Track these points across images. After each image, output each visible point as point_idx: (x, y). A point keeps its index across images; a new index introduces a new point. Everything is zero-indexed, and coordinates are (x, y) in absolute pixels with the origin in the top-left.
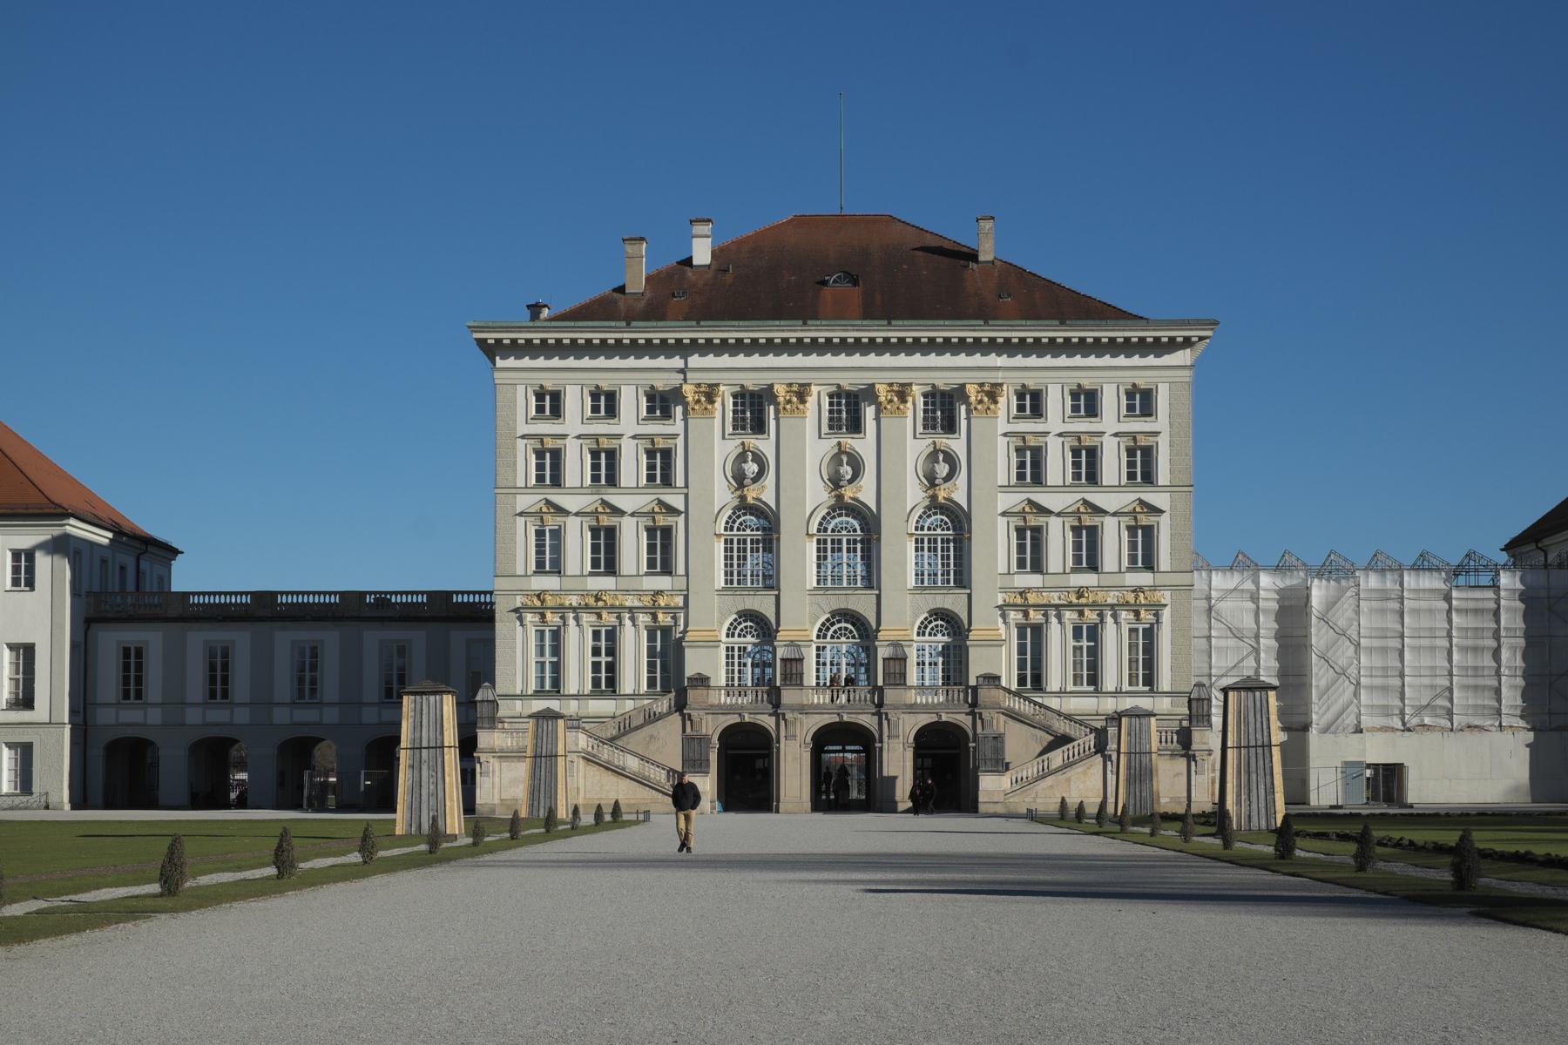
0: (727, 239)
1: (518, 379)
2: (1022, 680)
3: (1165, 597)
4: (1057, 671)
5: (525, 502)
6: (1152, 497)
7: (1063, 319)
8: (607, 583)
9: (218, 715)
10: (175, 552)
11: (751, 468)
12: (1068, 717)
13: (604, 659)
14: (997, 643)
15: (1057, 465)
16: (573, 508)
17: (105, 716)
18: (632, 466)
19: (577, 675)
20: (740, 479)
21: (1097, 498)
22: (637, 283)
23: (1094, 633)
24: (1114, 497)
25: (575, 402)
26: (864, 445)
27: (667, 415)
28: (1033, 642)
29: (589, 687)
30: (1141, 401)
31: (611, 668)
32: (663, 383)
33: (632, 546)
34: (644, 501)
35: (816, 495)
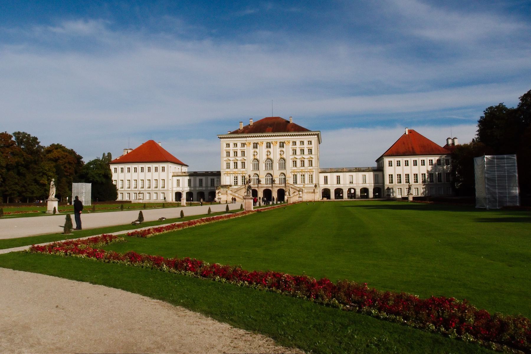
1: (224, 142)
3: (314, 170)
6: (312, 156)
7: (298, 131)
8: (236, 170)
9: (201, 189)
11: (256, 153)
14: (290, 177)
15: (298, 152)
18: (239, 154)
20: (254, 155)
22: (242, 128)
23: (304, 176)
24: (306, 156)
25: (232, 145)
26: (271, 150)
28: (295, 176)
30: (310, 142)
32: (243, 142)
33: (239, 165)
34: (241, 158)
35: (265, 157)
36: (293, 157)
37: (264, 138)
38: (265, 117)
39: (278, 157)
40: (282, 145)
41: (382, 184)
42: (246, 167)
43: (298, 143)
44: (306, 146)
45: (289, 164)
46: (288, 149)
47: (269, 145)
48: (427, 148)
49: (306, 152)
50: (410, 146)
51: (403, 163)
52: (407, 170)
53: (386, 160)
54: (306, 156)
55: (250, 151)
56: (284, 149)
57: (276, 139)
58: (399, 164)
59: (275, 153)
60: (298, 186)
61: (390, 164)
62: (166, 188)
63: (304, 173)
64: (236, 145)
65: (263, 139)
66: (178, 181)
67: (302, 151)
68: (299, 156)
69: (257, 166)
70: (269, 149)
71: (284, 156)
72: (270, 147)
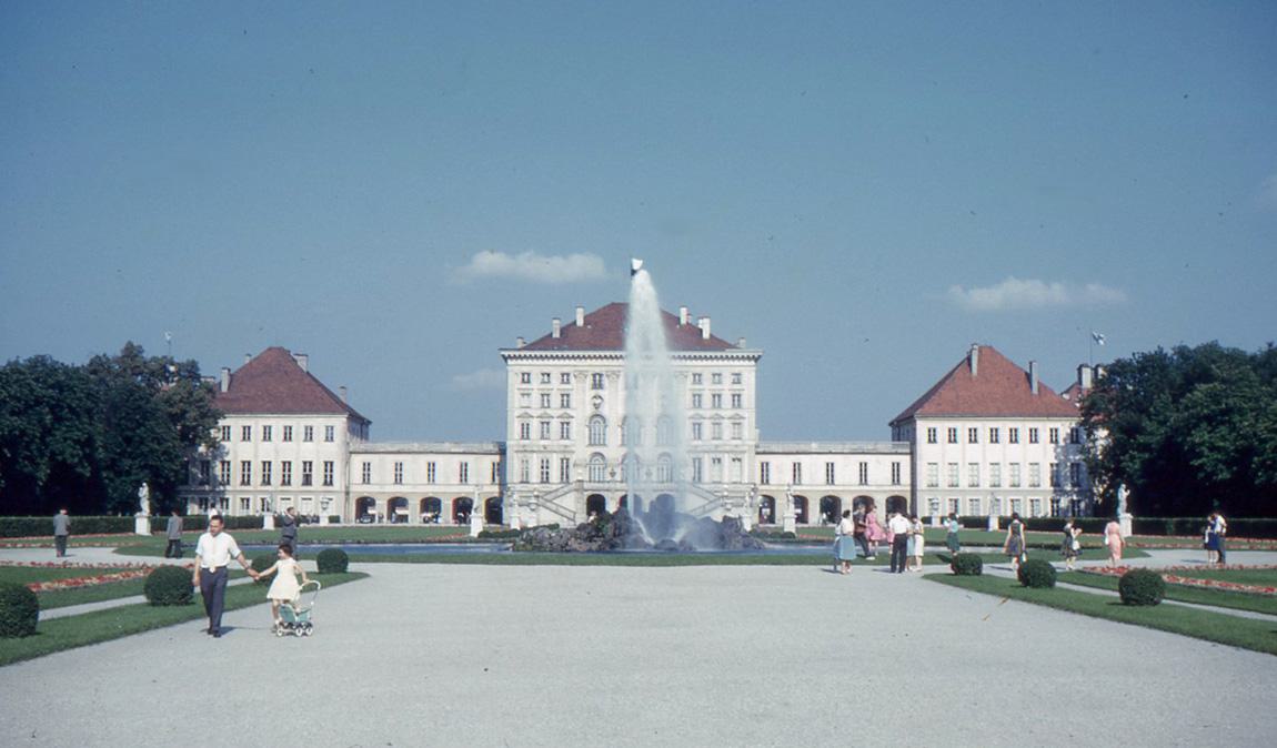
0: (588, 313)
2: (694, 478)
5: (516, 414)
10: (369, 422)
12: (708, 492)
13: (545, 470)
15: (707, 400)
16: (535, 415)
17: (353, 489)
19: (535, 476)
20: (595, 405)
21: (723, 413)
24: (727, 410)
27: (568, 382)
29: (539, 480)
31: (547, 473)
38: (609, 303)
41: (909, 488)
42: (573, 435)
43: (707, 376)
50: (984, 387)
51: (963, 435)
53: (922, 427)
58: (953, 438)
60: (706, 487)
61: (932, 440)
63: (719, 456)
66: (367, 467)
67: (717, 396)
68: (707, 411)
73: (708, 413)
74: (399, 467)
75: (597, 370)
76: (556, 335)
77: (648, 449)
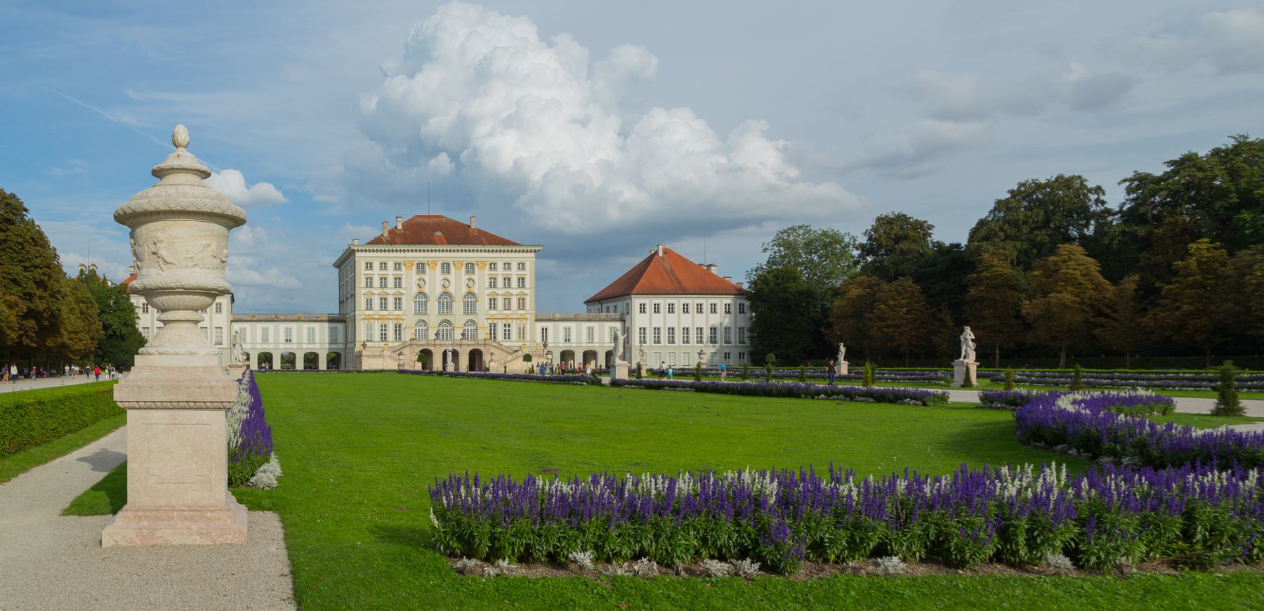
4: (500, 336)
5: (364, 291)
15: (500, 283)
18: (391, 282)
19: (377, 337)
24: (515, 290)
25: (376, 265)
26: (451, 277)
30: (522, 266)
35: (439, 290)
36: (491, 290)
37: (437, 254)
39: (464, 290)
40: (470, 268)
42: (404, 307)
43: (500, 266)
44: (514, 273)
45: (483, 305)
46: (482, 276)
47: (446, 268)
48: (700, 282)
49: (514, 282)
51: (678, 308)
52: (672, 320)
54: (515, 290)
55: (410, 278)
56: (475, 277)
57: (459, 255)
59: (458, 283)
61: (643, 309)
62: (224, 345)
64: (384, 265)
65: (435, 255)
67: (507, 280)
68: (500, 290)
69: (421, 307)
70: (448, 276)
71: (476, 290)
72: (448, 272)
73: (501, 292)
74: (265, 331)
75: (422, 260)
76: (386, 234)
77: (459, 317)
